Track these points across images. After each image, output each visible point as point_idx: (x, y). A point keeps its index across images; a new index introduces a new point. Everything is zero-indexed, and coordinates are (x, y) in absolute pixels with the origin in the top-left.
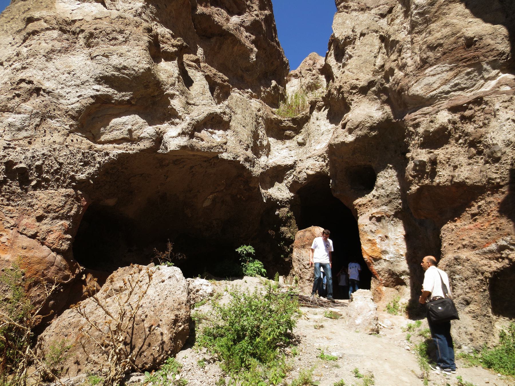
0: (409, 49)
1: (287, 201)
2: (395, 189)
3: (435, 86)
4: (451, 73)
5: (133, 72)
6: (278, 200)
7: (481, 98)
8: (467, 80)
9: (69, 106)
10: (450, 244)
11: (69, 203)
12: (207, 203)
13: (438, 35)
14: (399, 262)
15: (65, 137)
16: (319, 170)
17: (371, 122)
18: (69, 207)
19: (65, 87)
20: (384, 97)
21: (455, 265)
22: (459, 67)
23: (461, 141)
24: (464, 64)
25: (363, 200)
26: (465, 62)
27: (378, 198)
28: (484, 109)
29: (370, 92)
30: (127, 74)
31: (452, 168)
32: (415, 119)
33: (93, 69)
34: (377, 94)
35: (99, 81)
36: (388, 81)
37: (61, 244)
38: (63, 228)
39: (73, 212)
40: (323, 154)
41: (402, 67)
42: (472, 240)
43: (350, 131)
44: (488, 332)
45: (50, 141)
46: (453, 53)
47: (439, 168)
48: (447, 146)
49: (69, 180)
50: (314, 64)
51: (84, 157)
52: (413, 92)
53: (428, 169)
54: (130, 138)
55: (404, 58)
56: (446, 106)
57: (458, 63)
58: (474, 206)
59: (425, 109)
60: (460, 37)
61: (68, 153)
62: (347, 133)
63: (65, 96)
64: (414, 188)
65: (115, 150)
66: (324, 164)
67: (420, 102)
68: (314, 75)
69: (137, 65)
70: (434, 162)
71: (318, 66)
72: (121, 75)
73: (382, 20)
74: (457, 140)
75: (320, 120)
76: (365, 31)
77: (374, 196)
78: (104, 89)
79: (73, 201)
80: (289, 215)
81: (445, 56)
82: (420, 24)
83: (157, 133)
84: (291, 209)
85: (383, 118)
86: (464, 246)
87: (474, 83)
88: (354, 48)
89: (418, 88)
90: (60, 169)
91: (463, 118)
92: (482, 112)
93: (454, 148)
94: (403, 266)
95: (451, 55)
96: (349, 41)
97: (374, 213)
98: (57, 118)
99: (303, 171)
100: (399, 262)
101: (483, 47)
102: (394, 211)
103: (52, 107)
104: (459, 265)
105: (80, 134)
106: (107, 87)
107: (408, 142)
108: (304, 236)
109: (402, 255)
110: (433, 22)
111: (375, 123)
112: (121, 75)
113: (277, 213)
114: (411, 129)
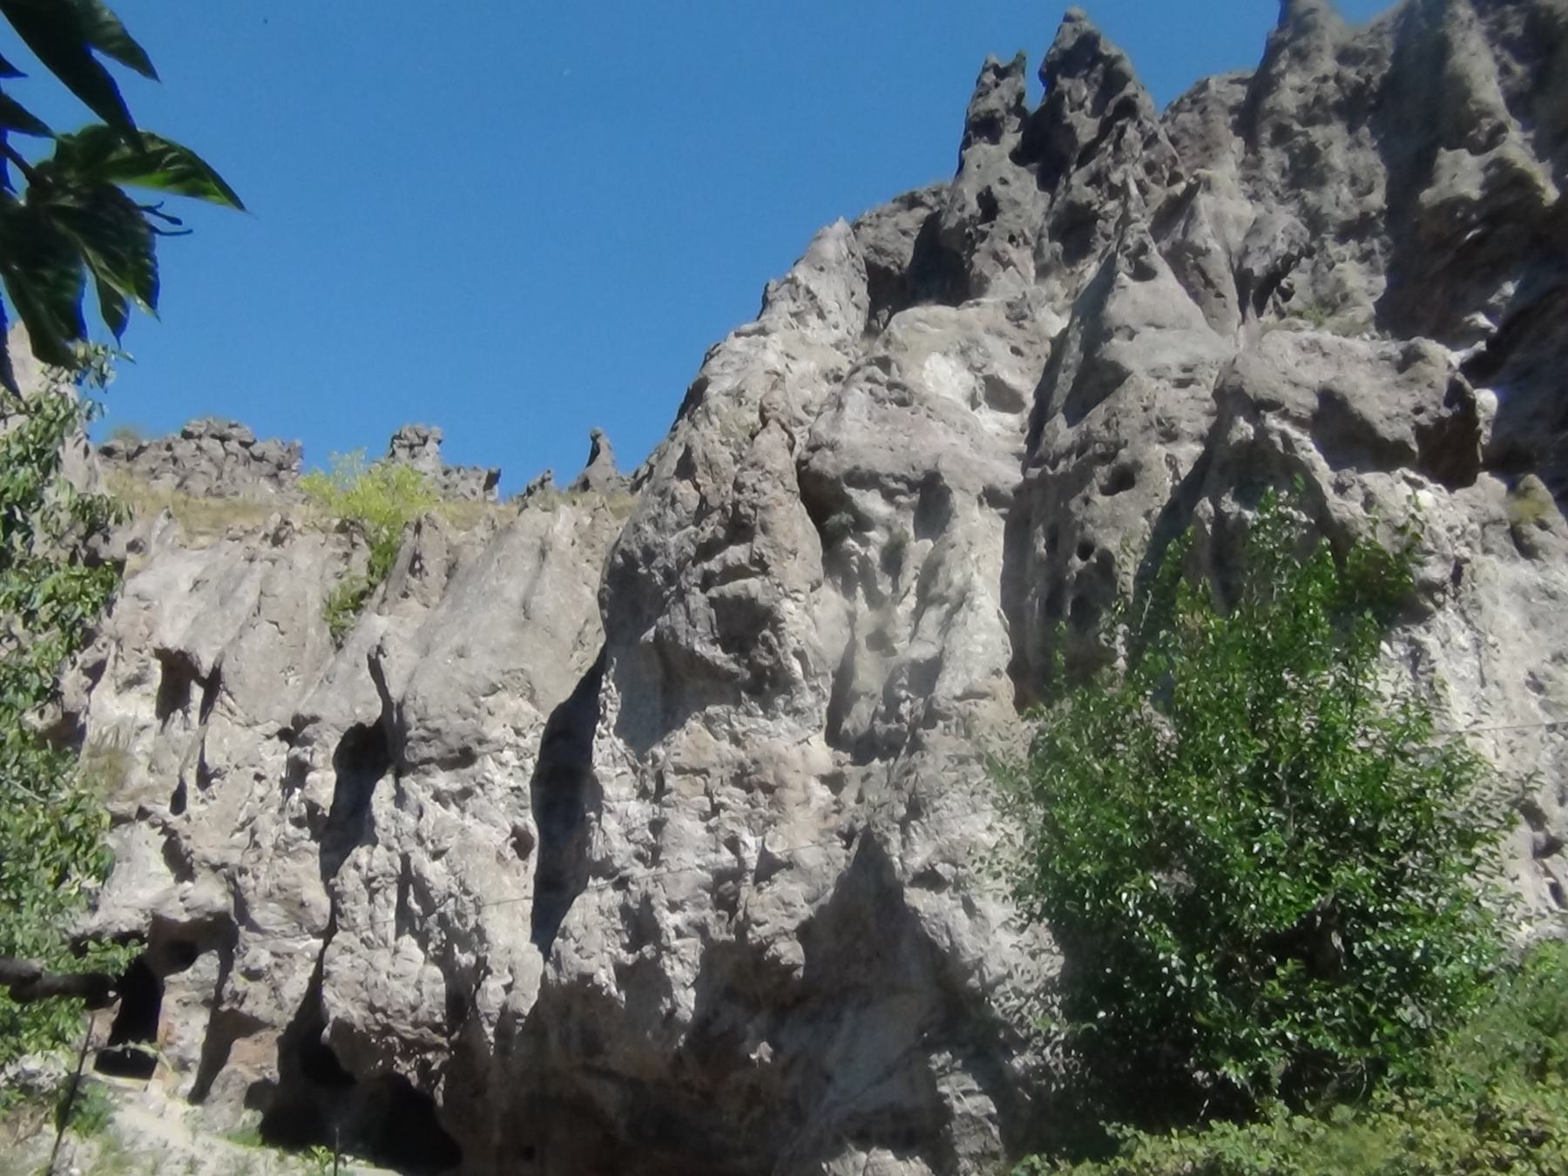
41: (256, 877)
43: (187, 910)
44: (236, 1119)
57: (291, 915)
59: (259, 937)
67: (253, 927)
73: (266, 743)
91: (276, 965)
94: (197, 1054)
96: (218, 774)
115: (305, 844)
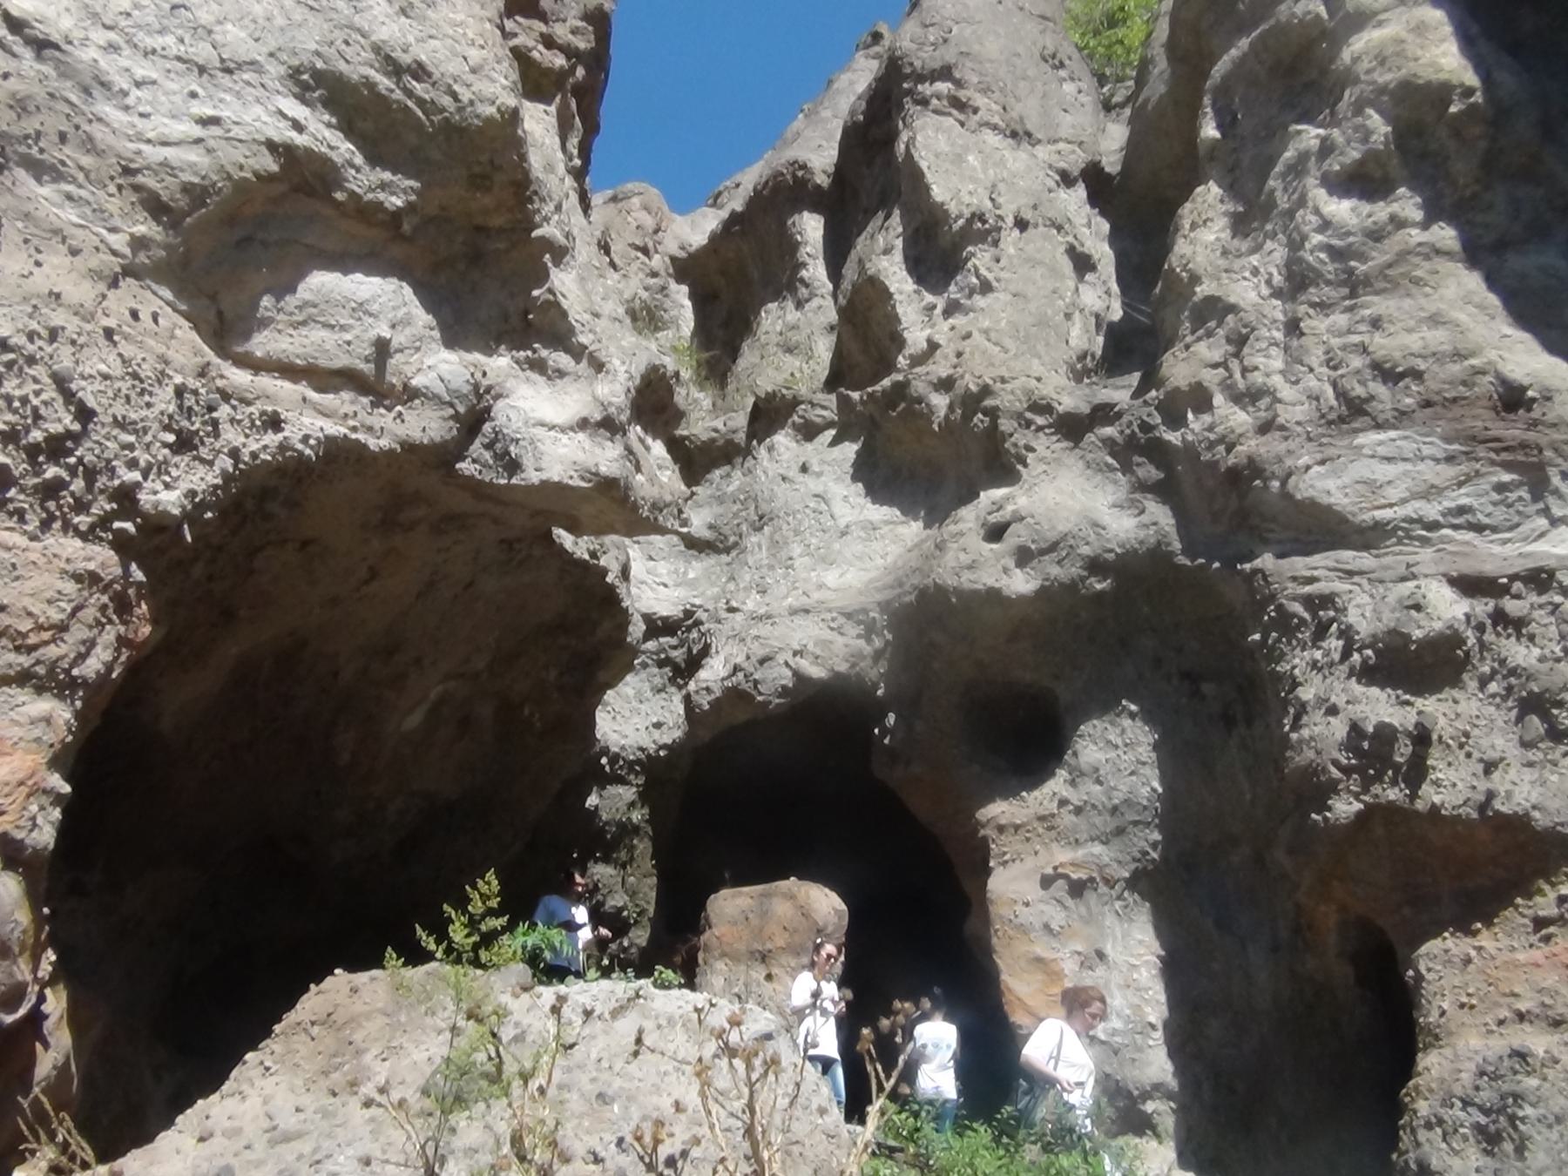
0: (1277, 345)
1: (638, 762)
2: (1145, 791)
3: (1393, 494)
4: (1449, 472)
5: (446, 101)
6: (605, 751)
7: (1551, 574)
8: (1495, 504)
9: (144, 147)
10: (1462, 1006)
11: (90, 614)
12: (414, 720)
13: (1414, 342)
14: (1140, 1050)
15: (102, 287)
16: (843, 667)
17: (1096, 544)
18: (86, 634)
19: (127, 51)
20: (1149, 471)
21: (1516, 1073)
22: (1477, 460)
23: (1493, 687)
24: (1493, 455)
25: (1013, 809)
26: (1497, 451)
27: (1078, 811)
28: (1557, 606)
29: (1090, 437)
30: (421, 102)
31: (1480, 768)
32: (1311, 580)
33: (280, 21)
34: (1125, 453)
35: (305, 87)
36: (1175, 420)
37: (33, 819)
38: (50, 737)
39: (92, 667)
40: (865, 611)
41: (1246, 397)
42: (1548, 1001)
43: (1024, 557)
45: (29, 285)
46: (1457, 411)
47: (1435, 758)
48: (1456, 693)
49: (103, 506)
50: (656, 231)
51: (180, 407)
52: (1311, 493)
53: (1403, 752)
54: (373, 382)
55: (1256, 368)
56: (1442, 569)
57: (1471, 445)
58: (1545, 895)
59: (1349, 557)
60: (1482, 372)
61: (117, 369)
62: (1011, 563)
63: (125, 94)
64: (1344, 808)
65: (312, 420)
66: (868, 650)
67: (1323, 529)
68: (654, 275)
69: (470, 78)
70: (1422, 738)
71: (672, 247)
72: (398, 95)
73: (1063, 194)
74: (1484, 682)
75: (819, 475)
76: (1028, 215)
77: (1063, 803)
78: (320, 133)
79: (103, 608)
80: (636, 816)
81: (1428, 411)
82: (1328, 283)
83: (476, 386)
84: (645, 796)
85: (1141, 543)
86: (1521, 1017)
87: (1516, 519)
88: (998, 261)
89: (1331, 484)
90: (76, 438)
92: (1552, 613)
93: (1474, 704)
94: (1157, 1065)
95: (1450, 415)
97: (1062, 865)
98: (74, 181)
99: (780, 659)
100: (1140, 1050)
101: (1555, 425)
102: (1133, 866)
103: (52, 123)
104: (1528, 1074)
105: (167, 294)
106: (329, 125)
107: (1273, 648)
108: (764, 915)
109: (1153, 1027)
110: (1377, 293)
111: (1111, 551)
112: (398, 95)
113: (592, 800)
114: (1297, 608)
115: (1416, 235)
